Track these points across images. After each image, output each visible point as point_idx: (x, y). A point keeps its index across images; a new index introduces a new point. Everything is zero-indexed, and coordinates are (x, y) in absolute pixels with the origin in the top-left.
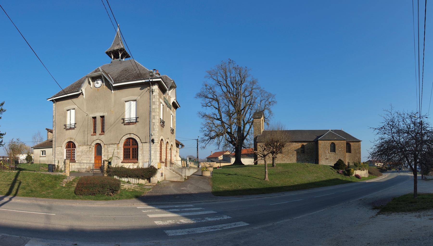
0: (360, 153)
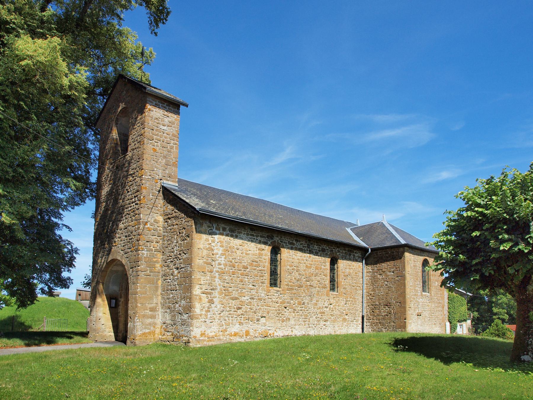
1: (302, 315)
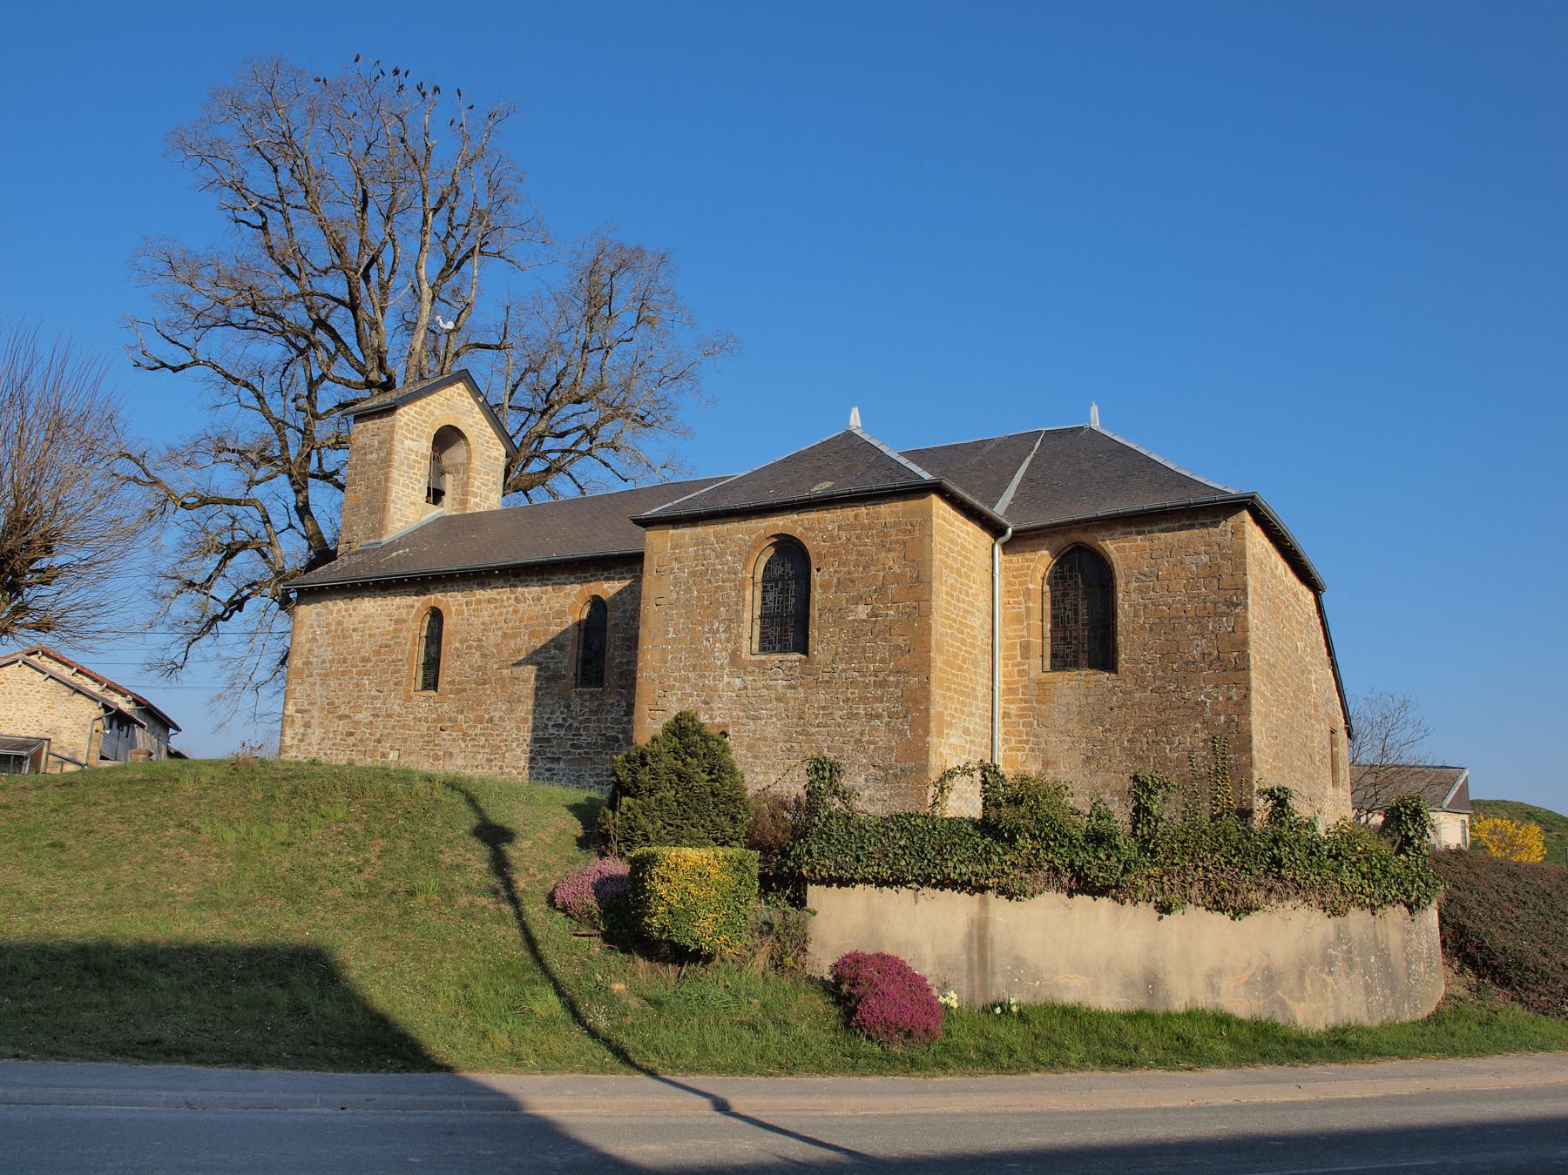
0: (1244, 656)
1: (483, 746)
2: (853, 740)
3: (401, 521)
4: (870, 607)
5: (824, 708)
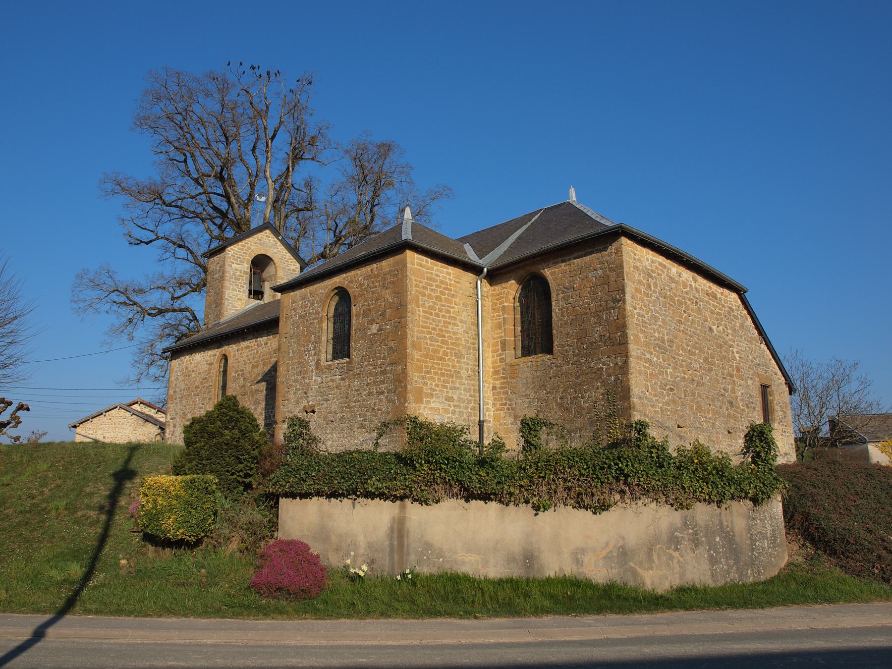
0: (625, 335)
2: (371, 409)
3: (233, 310)
4: (378, 325)
5: (357, 390)
